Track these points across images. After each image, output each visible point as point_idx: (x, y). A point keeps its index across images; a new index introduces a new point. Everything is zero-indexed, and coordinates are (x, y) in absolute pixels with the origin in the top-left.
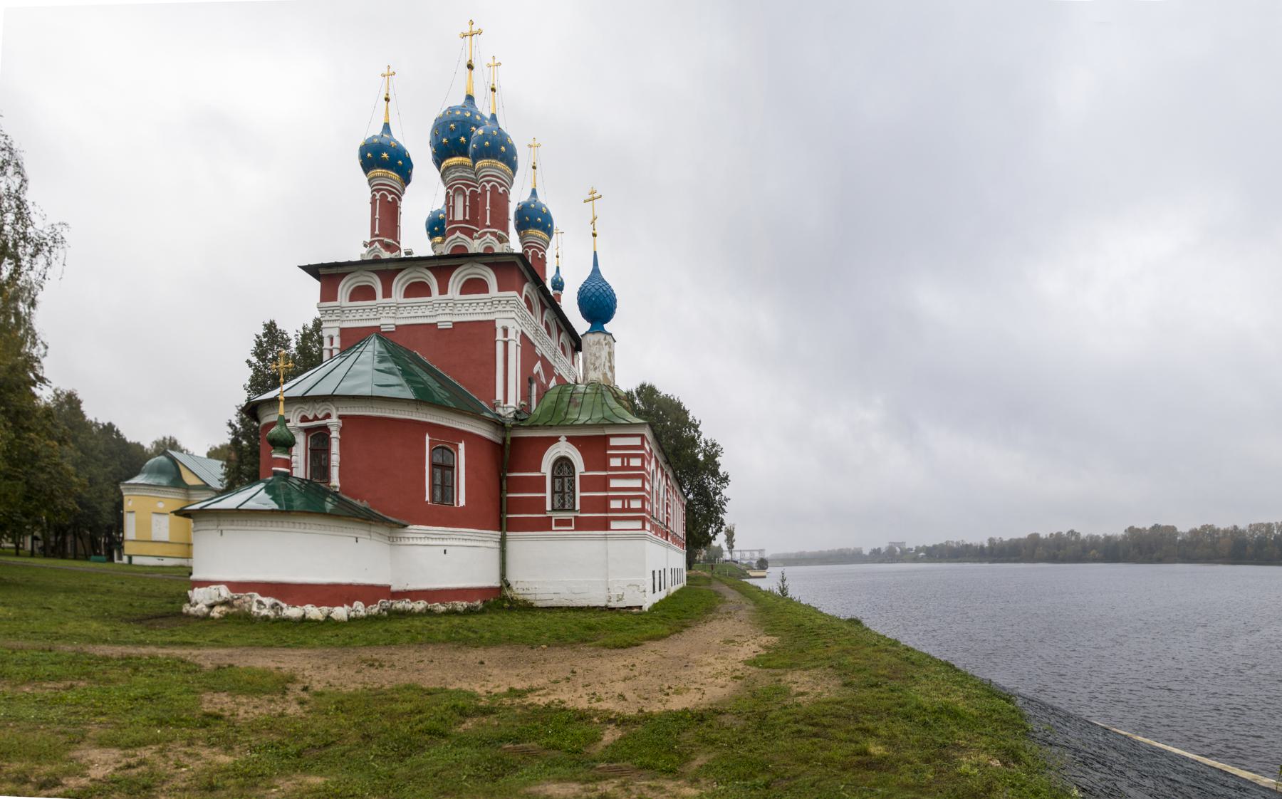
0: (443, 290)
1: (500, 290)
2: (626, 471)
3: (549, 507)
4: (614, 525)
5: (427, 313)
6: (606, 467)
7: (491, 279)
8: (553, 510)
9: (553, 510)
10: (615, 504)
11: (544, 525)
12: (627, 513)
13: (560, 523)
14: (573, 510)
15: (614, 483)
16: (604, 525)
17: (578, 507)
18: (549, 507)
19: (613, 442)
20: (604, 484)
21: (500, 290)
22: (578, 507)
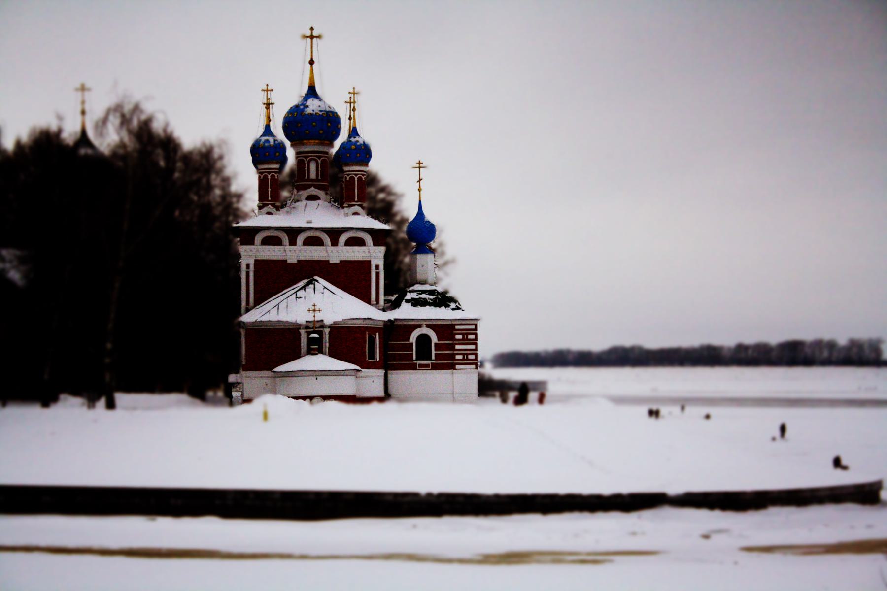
0: (335, 243)
1: (374, 245)
2: (465, 341)
3: (414, 358)
4: (457, 367)
5: (322, 254)
6: (454, 339)
7: (368, 239)
8: (418, 359)
9: (418, 359)
10: (458, 357)
11: (413, 367)
12: (466, 361)
13: (420, 366)
14: (430, 358)
15: (457, 347)
16: (452, 367)
17: (433, 358)
18: (414, 358)
19: (457, 327)
20: (452, 347)
21: (374, 245)
22: (433, 358)
